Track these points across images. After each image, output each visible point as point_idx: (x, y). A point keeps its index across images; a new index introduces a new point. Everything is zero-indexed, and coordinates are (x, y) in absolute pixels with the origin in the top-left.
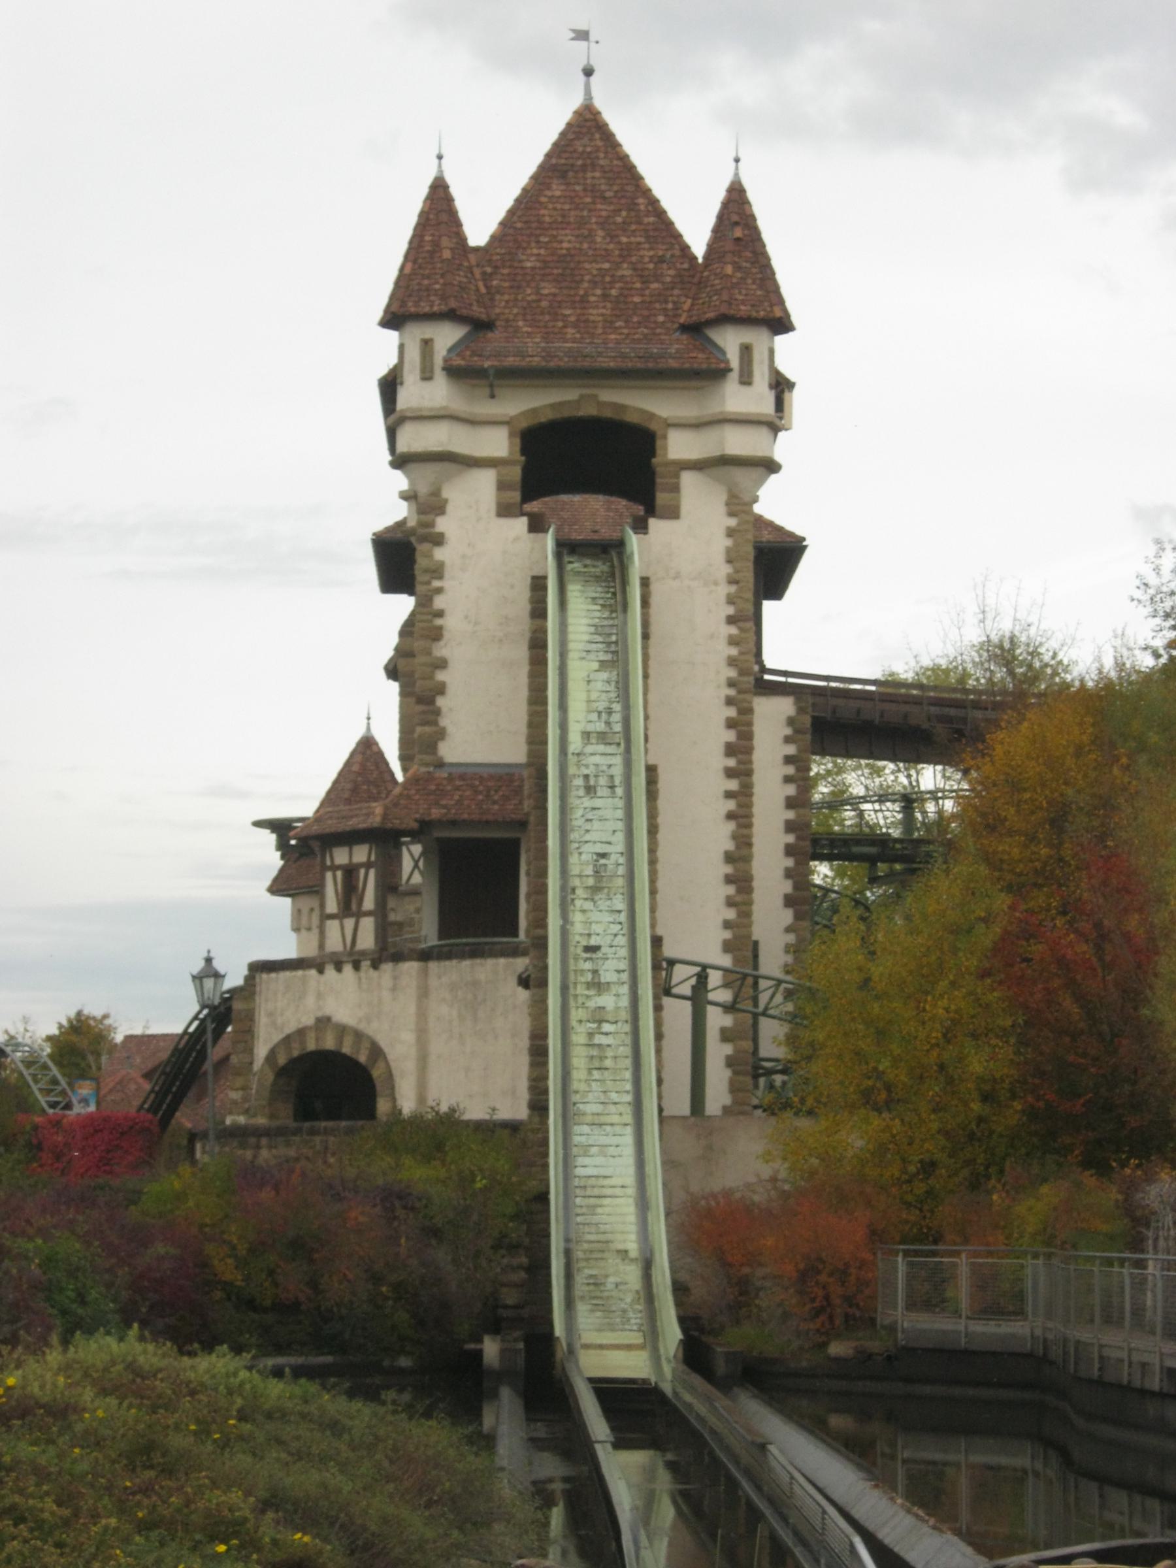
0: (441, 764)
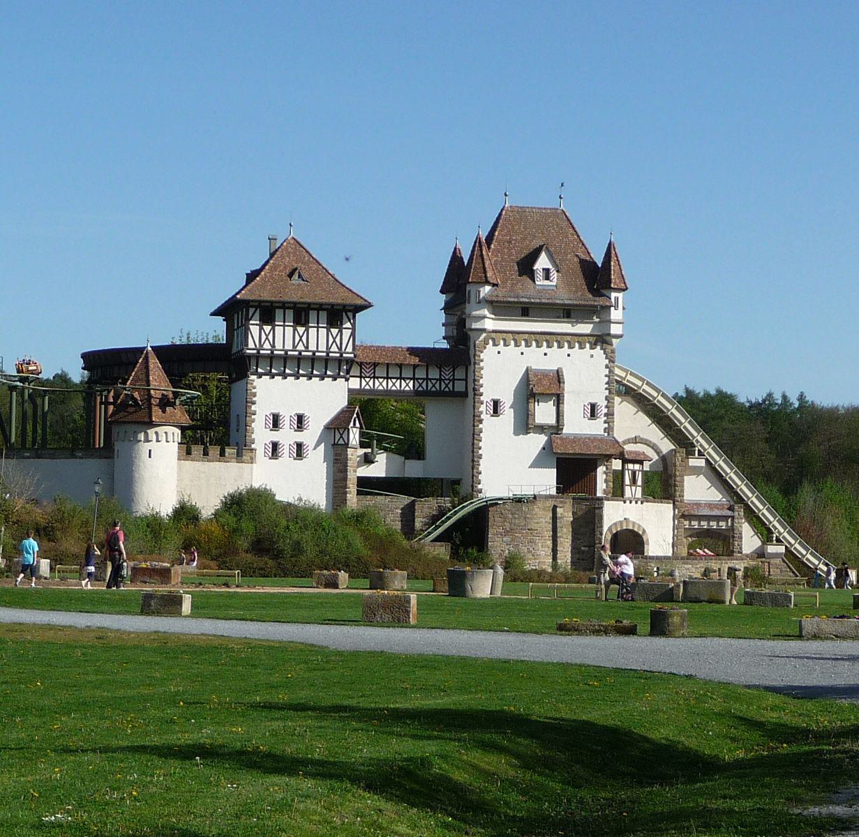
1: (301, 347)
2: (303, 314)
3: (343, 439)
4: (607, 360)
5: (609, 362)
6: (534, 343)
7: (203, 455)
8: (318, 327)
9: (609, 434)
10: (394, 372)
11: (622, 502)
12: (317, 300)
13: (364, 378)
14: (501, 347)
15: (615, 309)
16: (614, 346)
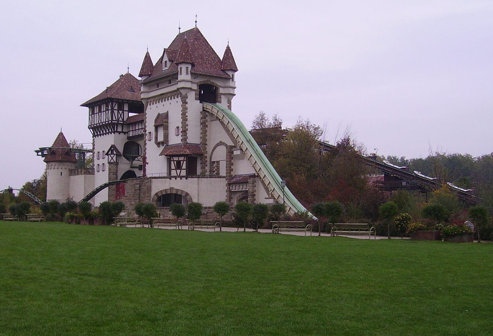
0: (187, 143)
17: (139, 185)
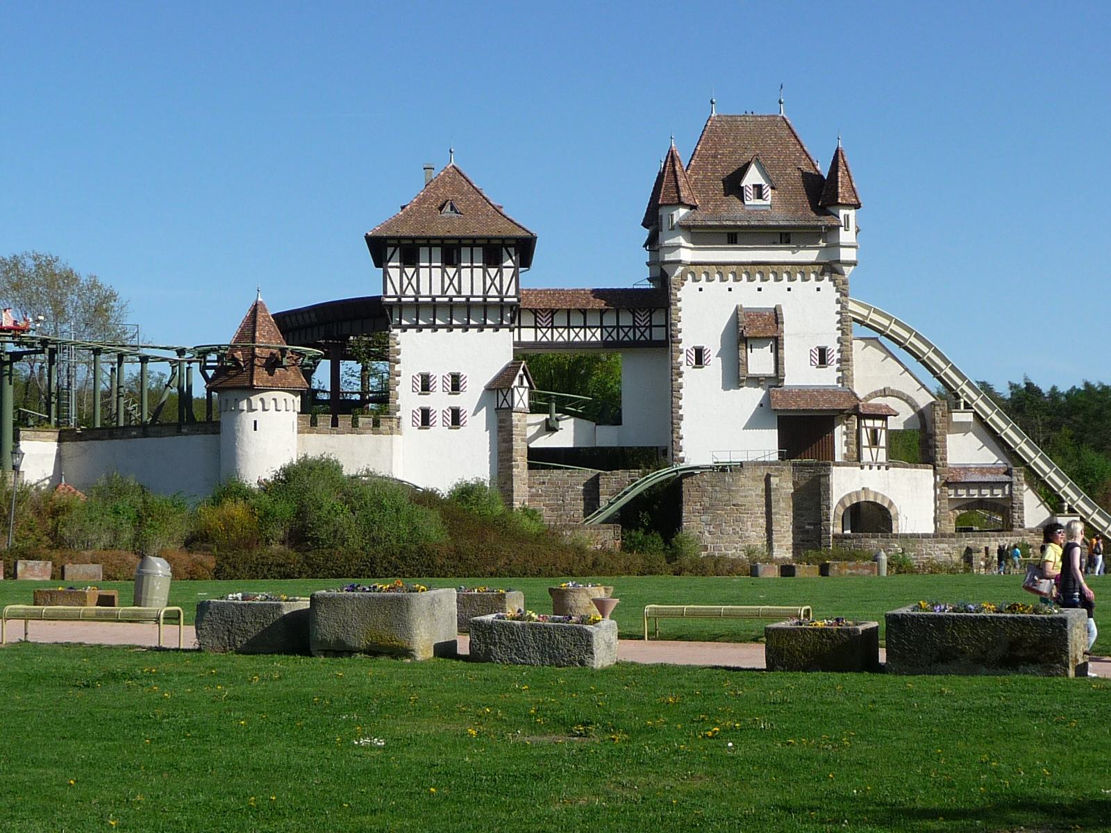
1: (451, 292)
2: (455, 252)
3: (507, 401)
4: (839, 294)
5: (841, 296)
6: (744, 276)
7: (332, 426)
8: (472, 268)
9: (843, 385)
10: (577, 320)
11: (859, 468)
12: (468, 233)
13: (540, 328)
14: (703, 282)
15: (845, 230)
16: (846, 276)
17: (778, 478)
